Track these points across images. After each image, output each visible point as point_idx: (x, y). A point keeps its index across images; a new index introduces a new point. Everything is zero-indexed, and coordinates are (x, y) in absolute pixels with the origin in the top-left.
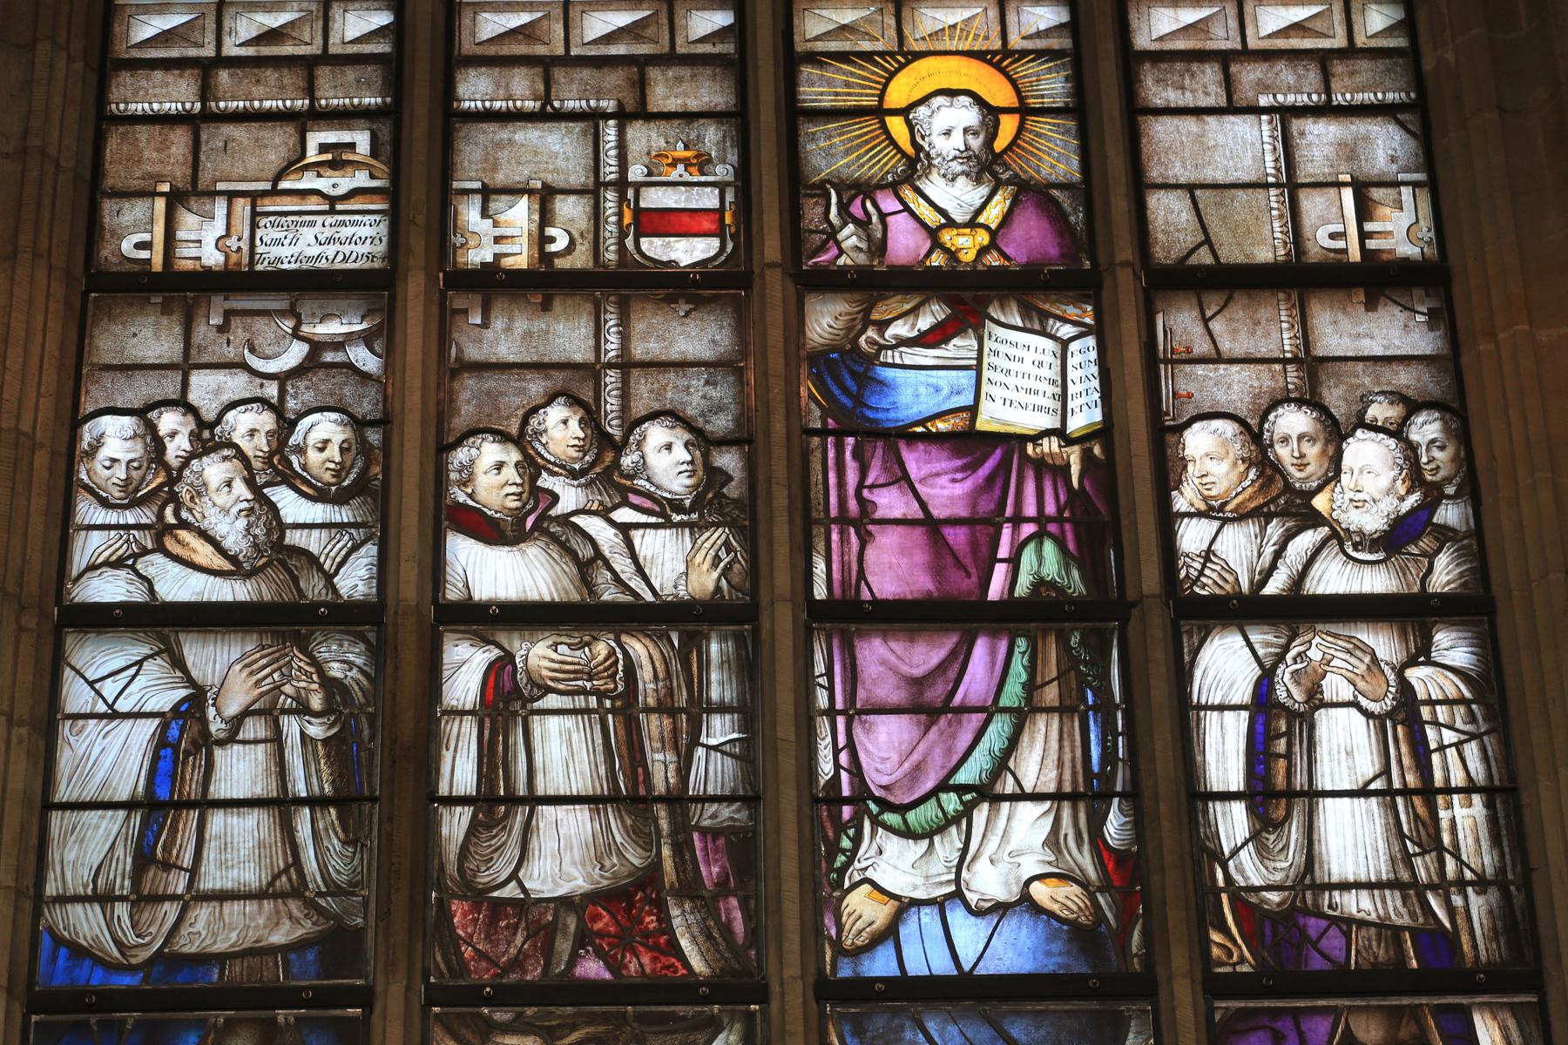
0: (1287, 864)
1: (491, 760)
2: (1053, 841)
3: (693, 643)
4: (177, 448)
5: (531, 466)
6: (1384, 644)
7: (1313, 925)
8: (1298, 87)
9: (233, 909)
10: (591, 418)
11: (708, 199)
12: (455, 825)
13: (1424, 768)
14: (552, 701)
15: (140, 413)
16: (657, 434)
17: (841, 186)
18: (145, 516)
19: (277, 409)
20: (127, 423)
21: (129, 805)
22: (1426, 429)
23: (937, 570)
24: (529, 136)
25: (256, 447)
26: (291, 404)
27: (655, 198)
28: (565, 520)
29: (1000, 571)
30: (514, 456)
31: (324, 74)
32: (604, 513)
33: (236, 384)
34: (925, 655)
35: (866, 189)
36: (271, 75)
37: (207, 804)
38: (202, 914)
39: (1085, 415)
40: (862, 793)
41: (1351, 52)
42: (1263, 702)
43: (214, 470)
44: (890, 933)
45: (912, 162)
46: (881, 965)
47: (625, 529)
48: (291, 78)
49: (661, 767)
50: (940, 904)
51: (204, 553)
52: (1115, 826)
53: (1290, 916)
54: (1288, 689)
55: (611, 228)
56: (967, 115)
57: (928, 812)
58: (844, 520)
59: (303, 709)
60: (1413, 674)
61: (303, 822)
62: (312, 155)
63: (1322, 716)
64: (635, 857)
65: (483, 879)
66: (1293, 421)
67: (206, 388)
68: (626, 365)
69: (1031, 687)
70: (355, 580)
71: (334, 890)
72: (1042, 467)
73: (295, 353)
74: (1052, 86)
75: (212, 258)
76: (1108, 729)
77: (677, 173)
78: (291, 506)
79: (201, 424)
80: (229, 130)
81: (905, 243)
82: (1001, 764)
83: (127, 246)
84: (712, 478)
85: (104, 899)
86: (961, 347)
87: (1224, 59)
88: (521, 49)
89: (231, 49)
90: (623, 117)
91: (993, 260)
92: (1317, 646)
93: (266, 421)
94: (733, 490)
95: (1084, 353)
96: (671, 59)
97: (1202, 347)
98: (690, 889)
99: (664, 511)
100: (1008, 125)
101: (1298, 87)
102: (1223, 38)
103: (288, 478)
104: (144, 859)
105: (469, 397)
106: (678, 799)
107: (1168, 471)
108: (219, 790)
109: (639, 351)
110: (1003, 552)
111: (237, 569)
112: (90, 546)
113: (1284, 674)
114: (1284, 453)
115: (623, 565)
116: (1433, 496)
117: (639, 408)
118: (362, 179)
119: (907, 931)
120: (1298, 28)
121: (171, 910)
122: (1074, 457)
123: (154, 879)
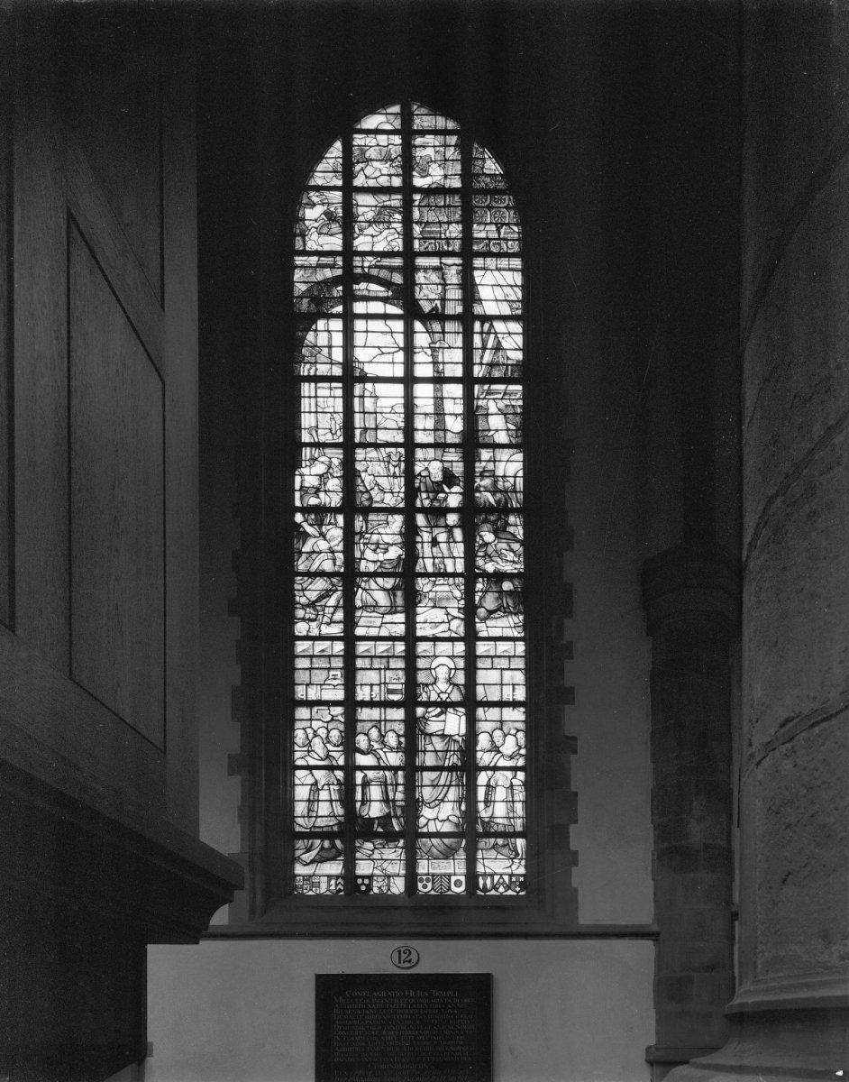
0: (489, 814)
1: (364, 794)
2: (453, 809)
3: (396, 773)
4: (311, 736)
5: (369, 740)
6: (509, 774)
7: (492, 824)
8: (504, 663)
9: (324, 819)
10: (380, 731)
11: (400, 687)
12: (358, 805)
13: (513, 797)
14: (373, 783)
15: (304, 729)
16: (391, 734)
17: (423, 684)
18: (306, 749)
19: (327, 728)
20: (302, 731)
21: (306, 801)
22: (520, 735)
23: (436, 761)
24: (369, 673)
25: (324, 736)
26: (329, 728)
27: (390, 687)
28: (375, 750)
29: (447, 761)
30: (366, 738)
31: (332, 659)
32: (381, 749)
33: (320, 724)
34: (434, 775)
35: (427, 685)
36: (323, 659)
37: (318, 801)
38: (319, 819)
39: (463, 731)
40: (423, 800)
41: (515, 656)
42: (488, 786)
43: (317, 740)
44: (427, 824)
45: (436, 679)
46: (425, 830)
47: (385, 752)
48: (327, 660)
49: (391, 796)
50: (434, 819)
51: (316, 757)
52: (463, 808)
53: (488, 823)
54: (492, 783)
55: (383, 693)
56: (445, 670)
57: (432, 805)
58: (422, 751)
59: (333, 784)
60: (513, 781)
61: (334, 803)
62: (331, 677)
63: (497, 788)
64: (387, 811)
65: (363, 814)
66: (498, 733)
67: (315, 724)
68: (385, 721)
69: (451, 781)
70: (341, 762)
71: (340, 816)
72: (455, 741)
73: (329, 718)
74: (461, 663)
75: (314, 698)
76: (463, 789)
77: (394, 681)
78: (330, 747)
79: (315, 731)
80: (315, 671)
81: (434, 697)
82: (445, 796)
83: (299, 696)
84: (400, 743)
85: (304, 817)
86: (442, 717)
87: (492, 657)
88: (367, 654)
89: (315, 654)
90: (385, 669)
91: (448, 700)
92: (499, 774)
93: (325, 731)
94: (403, 745)
95: (464, 718)
96: (394, 656)
97: (483, 719)
98: (396, 817)
99: (391, 749)
100: (453, 671)
101: (504, 663)
102: (492, 653)
103: (329, 742)
104: (309, 810)
105: (359, 726)
106: (394, 801)
107: (475, 743)
108: (321, 798)
109: (387, 718)
110: (448, 757)
111: (322, 760)
112: (297, 755)
113: (492, 780)
114: (495, 739)
115: (384, 759)
116: (520, 748)
117: (388, 729)
118: (338, 682)
119: (429, 824)
120: (506, 651)
121: (314, 819)
122: (460, 739)
123: (311, 814)
